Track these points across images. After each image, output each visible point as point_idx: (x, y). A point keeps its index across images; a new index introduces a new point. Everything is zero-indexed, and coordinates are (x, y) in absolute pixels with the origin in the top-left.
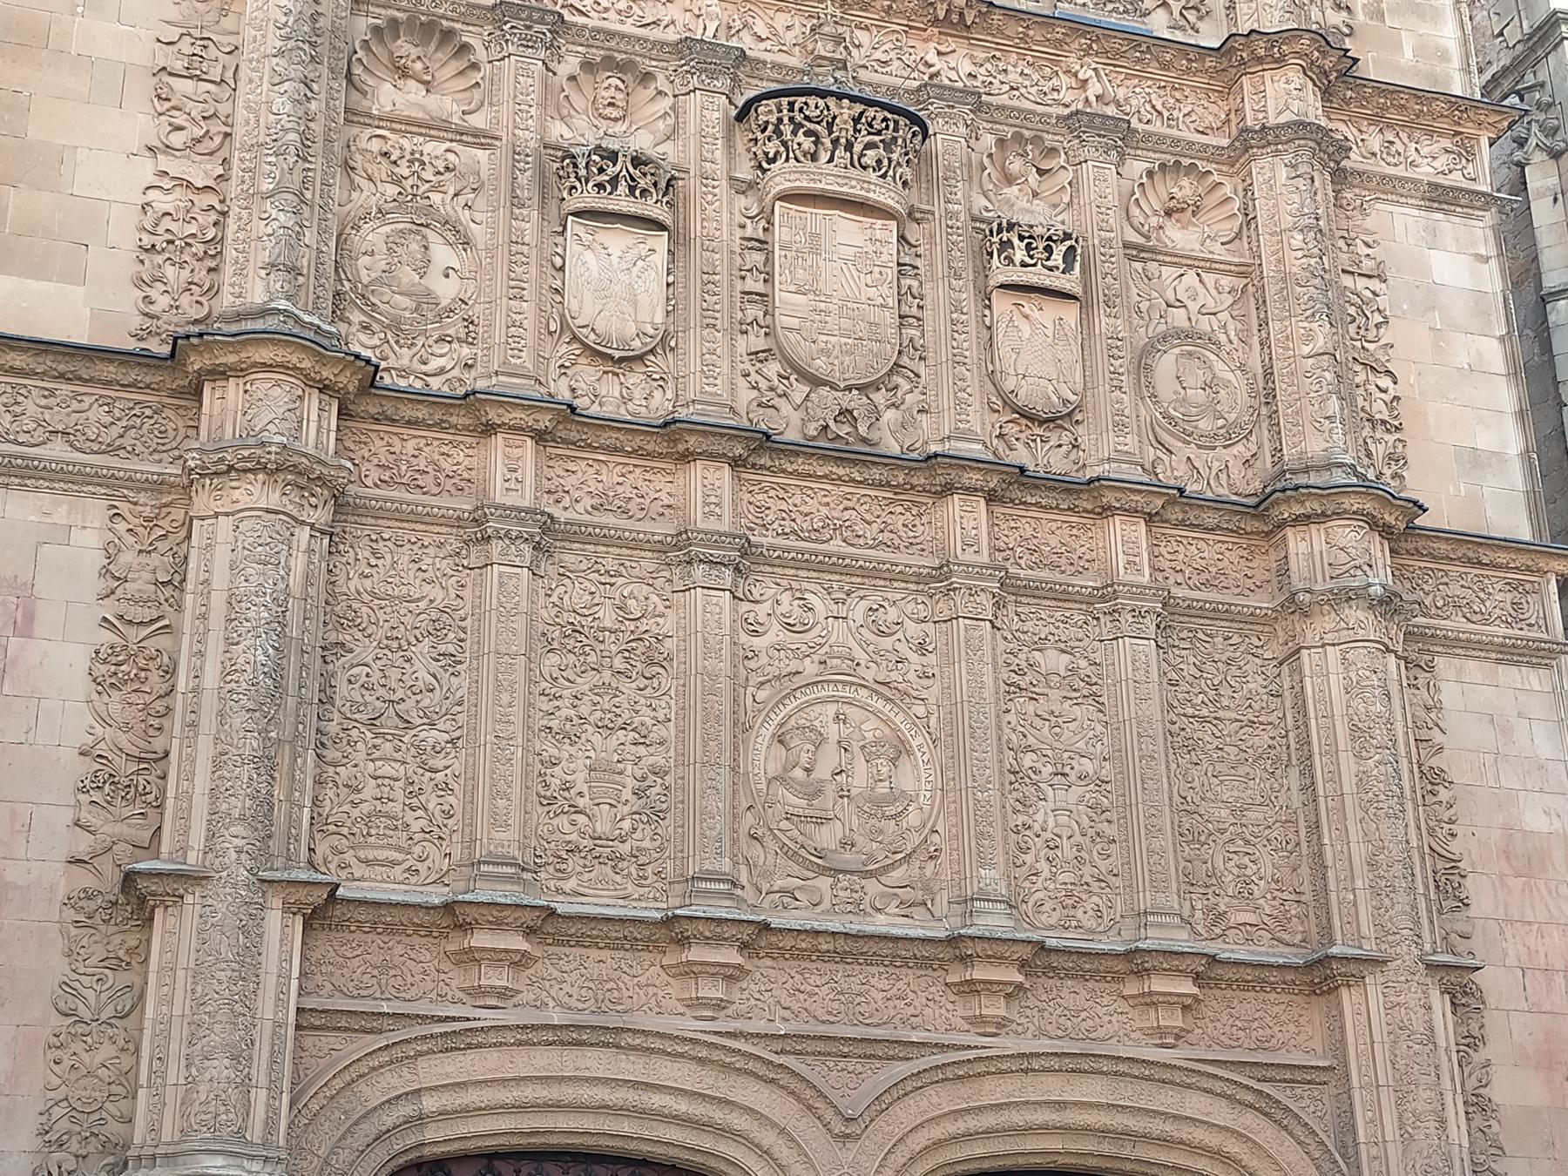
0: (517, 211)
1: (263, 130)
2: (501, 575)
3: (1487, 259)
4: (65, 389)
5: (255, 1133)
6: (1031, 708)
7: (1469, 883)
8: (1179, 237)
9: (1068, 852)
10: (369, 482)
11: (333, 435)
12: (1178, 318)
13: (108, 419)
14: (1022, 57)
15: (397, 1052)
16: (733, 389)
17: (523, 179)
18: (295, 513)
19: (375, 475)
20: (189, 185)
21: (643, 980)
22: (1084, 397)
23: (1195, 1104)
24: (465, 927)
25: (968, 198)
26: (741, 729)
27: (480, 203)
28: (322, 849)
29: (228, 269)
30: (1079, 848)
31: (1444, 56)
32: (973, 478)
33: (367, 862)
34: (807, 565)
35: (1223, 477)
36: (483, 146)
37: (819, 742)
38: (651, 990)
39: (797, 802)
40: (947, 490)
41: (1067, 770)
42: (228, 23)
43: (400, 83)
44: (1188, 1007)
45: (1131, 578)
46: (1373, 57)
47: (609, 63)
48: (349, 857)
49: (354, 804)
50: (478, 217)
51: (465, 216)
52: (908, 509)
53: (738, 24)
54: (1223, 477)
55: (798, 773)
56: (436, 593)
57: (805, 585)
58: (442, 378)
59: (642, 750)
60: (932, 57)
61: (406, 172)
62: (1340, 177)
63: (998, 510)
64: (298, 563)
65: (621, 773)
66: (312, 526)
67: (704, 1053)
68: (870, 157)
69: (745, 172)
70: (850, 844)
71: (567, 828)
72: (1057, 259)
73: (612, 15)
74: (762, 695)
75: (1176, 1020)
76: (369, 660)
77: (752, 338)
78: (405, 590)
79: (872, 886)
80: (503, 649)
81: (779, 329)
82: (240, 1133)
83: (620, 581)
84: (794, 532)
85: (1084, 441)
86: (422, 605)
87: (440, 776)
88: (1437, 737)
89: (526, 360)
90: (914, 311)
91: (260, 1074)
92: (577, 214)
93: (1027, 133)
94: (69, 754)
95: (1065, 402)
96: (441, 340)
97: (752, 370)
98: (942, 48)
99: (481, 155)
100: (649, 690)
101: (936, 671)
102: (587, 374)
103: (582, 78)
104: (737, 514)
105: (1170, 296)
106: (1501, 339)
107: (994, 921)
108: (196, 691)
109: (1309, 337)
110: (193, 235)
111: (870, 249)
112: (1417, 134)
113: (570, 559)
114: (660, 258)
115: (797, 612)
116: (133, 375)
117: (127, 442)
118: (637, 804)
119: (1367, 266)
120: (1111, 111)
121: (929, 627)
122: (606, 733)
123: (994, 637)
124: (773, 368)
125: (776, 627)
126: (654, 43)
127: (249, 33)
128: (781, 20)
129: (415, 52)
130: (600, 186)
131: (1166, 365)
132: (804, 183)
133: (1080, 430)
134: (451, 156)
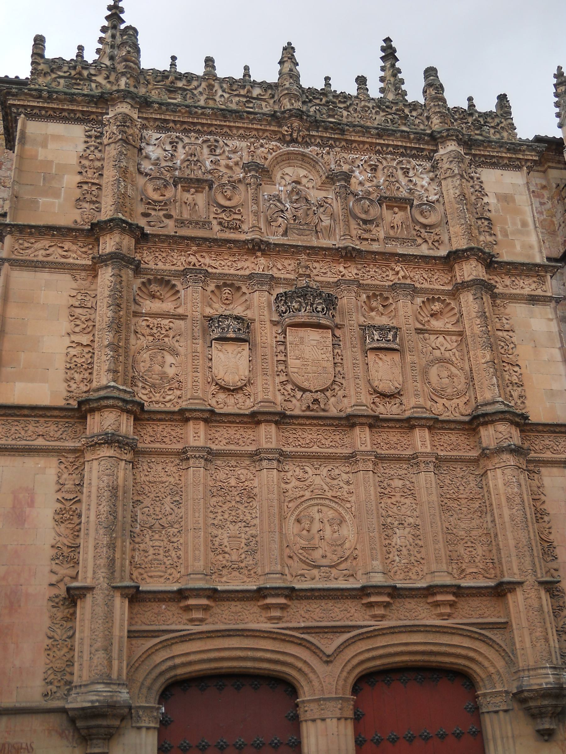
0: (194, 341)
1: (104, 324)
2: (193, 471)
3: (552, 320)
4: (42, 420)
5: (114, 676)
6: (389, 501)
8: (436, 324)
10: (146, 442)
11: (132, 427)
12: (437, 353)
13: (56, 429)
14: (375, 265)
15: (165, 644)
16: (275, 396)
17: (196, 330)
18: (119, 457)
19: (149, 439)
20: (82, 345)
21: (251, 611)
22: (403, 385)
24: (186, 598)
25: (357, 318)
26: (283, 518)
27: (182, 339)
28: (136, 574)
29: (95, 373)
30: (409, 551)
31: (531, 247)
32: (364, 420)
33: (151, 577)
34: (304, 457)
35: (457, 410)
36: (182, 319)
37: (312, 520)
38: (255, 615)
39: (303, 543)
41: (403, 522)
42: (93, 287)
43: (153, 300)
45: (423, 450)
46: (506, 252)
47: (225, 285)
48: (145, 576)
49: (146, 557)
50: (181, 344)
51: (177, 344)
52: (341, 433)
53: (271, 265)
54: (457, 410)
55: (305, 532)
56: (171, 479)
57: (304, 464)
58: (171, 403)
59: (247, 529)
60: (342, 269)
61: (155, 331)
62: (494, 296)
63: (374, 430)
64: (121, 474)
65: (240, 538)
66: (126, 460)
67: (274, 636)
68: (319, 308)
69: (276, 318)
70: (324, 557)
71: (221, 559)
72: (390, 337)
73: (226, 267)
74: (290, 505)
76: (149, 505)
77: (281, 377)
78: (160, 479)
79: (334, 572)
80: (195, 497)
81: (290, 374)
82: (109, 676)
83: (237, 469)
84: (299, 445)
85: (404, 401)
86: (167, 484)
87: (175, 545)
89: (200, 394)
90: (340, 361)
91: (115, 654)
92: (216, 339)
93: (378, 293)
94: (47, 547)
95: (397, 388)
96: (170, 389)
97: (282, 388)
98: (345, 266)
99: (182, 322)
100: (249, 508)
101: (354, 491)
102: (222, 396)
103: (216, 292)
104: (278, 441)
105: (434, 347)
106: (560, 348)
108: (88, 522)
109: (484, 356)
110: (84, 362)
111: (322, 340)
112: (523, 277)
113: (219, 462)
114: (246, 352)
115: (302, 474)
116: (64, 413)
117: (64, 436)
118: (246, 548)
119: (507, 327)
120: (408, 281)
121: (350, 475)
122: (234, 524)
123: (374, 476)
124: (289, 387)
125: (294, 480)
126: (241, 276)
127: (99, 290)
128: (286, 262)
129: (156, 289)
130: (223, 329)
131: (434, 371)
132: (297, 320)
133: (402, 398)
134: (171, 324)
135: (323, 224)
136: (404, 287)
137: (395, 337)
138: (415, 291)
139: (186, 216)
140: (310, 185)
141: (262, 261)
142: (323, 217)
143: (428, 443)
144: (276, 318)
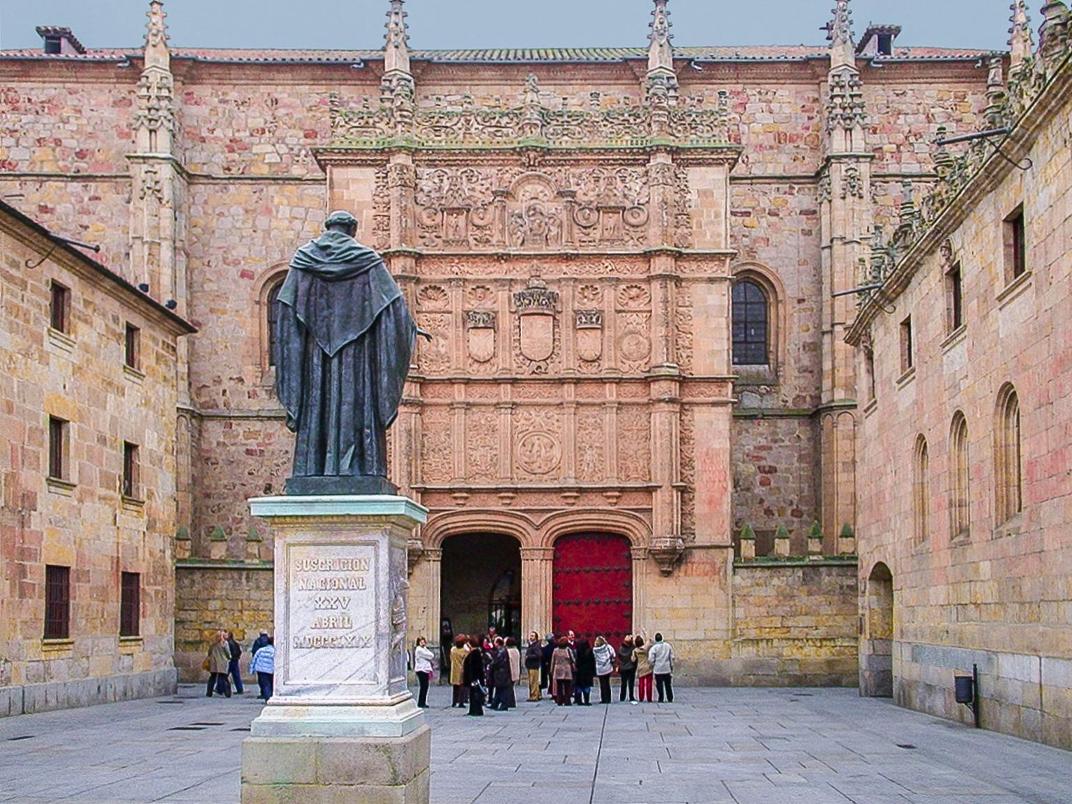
7: (695, 464)
9: (591, 465)
16: (511, 364)
23: (618, 518)
39: (527, 460)
40: (563, 383)
44: (617, 497)
60: (564, 268)
70: (540, 467)
72: (594, 320)
75: (615, 501)
79: (545, 477)
88: (692, 428)
107: (571, 483)
131: (626, 341)
132: (527, 312)
135: (552, 234)
136: (610, 279)
137: (597, 320)
138: (618, 279)
139: (451, 237)
140: (545, 198)
141: (505, 266)
142: (552, 228)
143: (615, 394)
144: (513, 310)
